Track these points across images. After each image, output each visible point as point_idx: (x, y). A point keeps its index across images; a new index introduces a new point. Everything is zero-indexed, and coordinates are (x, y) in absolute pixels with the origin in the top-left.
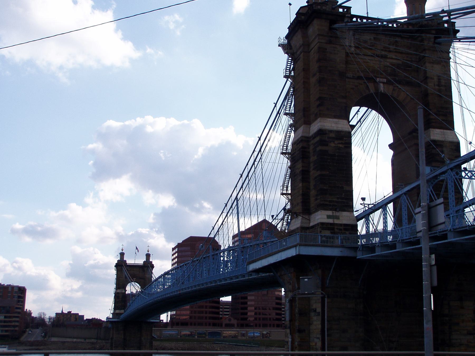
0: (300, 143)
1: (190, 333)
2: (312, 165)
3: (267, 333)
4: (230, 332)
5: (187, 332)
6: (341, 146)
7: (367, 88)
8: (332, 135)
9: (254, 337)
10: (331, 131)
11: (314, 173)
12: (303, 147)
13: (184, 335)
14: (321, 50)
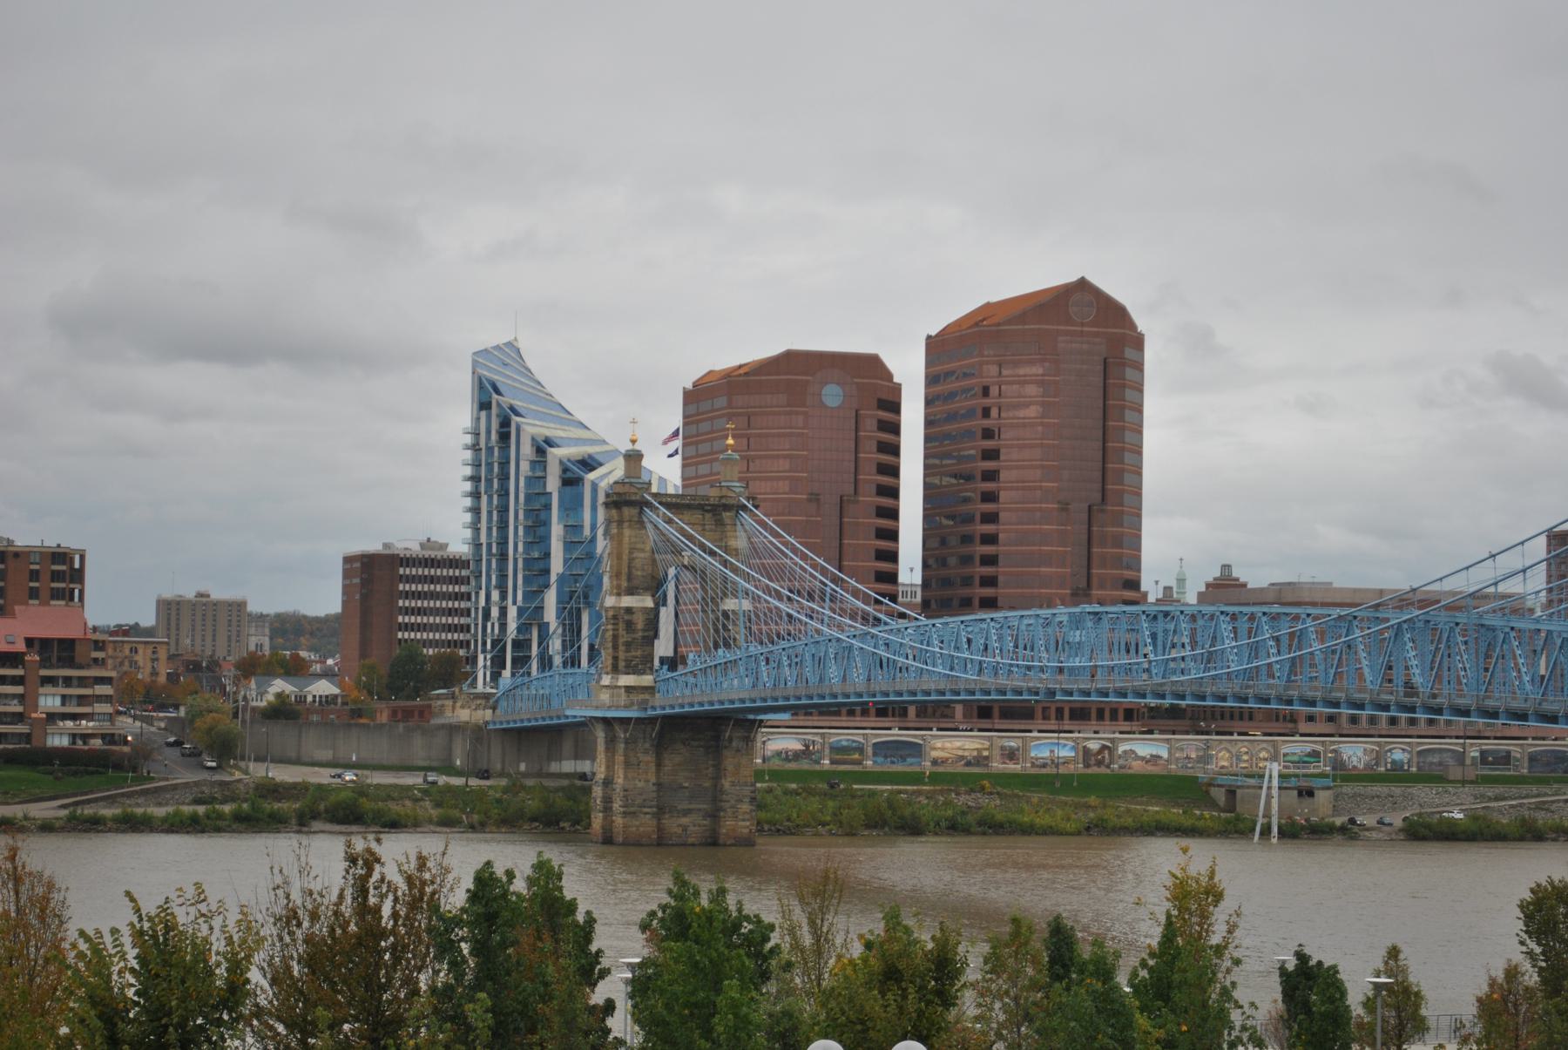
1: (799, 747)
3: (1104, 747)
4: (958, 744)
5: (794, 744)
9: (1055, 763)
13: (779, 754)
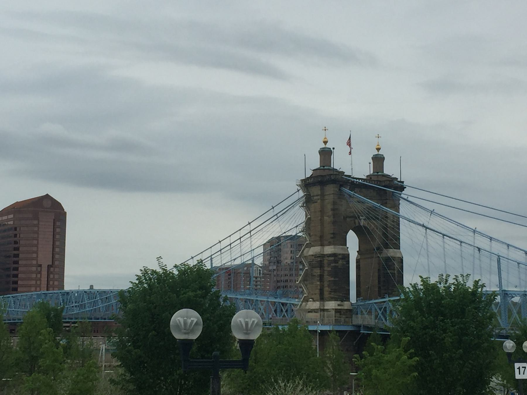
0: (318, 257)
2: (326, 272)
6: (345, 263)
7: (355, 223)
8: (340, 257)
10: (340, 254)
11: (327, 278)
12: (321, 261)
14: (334, 203)
